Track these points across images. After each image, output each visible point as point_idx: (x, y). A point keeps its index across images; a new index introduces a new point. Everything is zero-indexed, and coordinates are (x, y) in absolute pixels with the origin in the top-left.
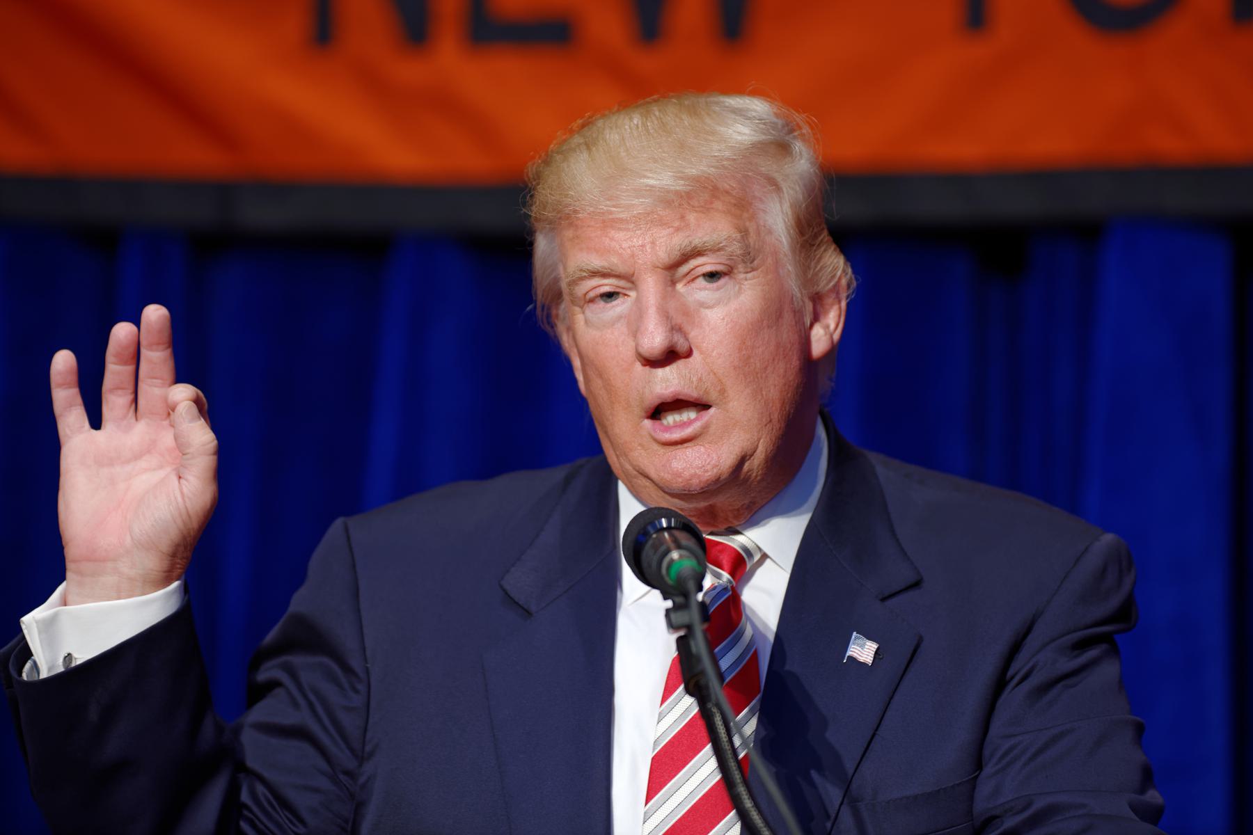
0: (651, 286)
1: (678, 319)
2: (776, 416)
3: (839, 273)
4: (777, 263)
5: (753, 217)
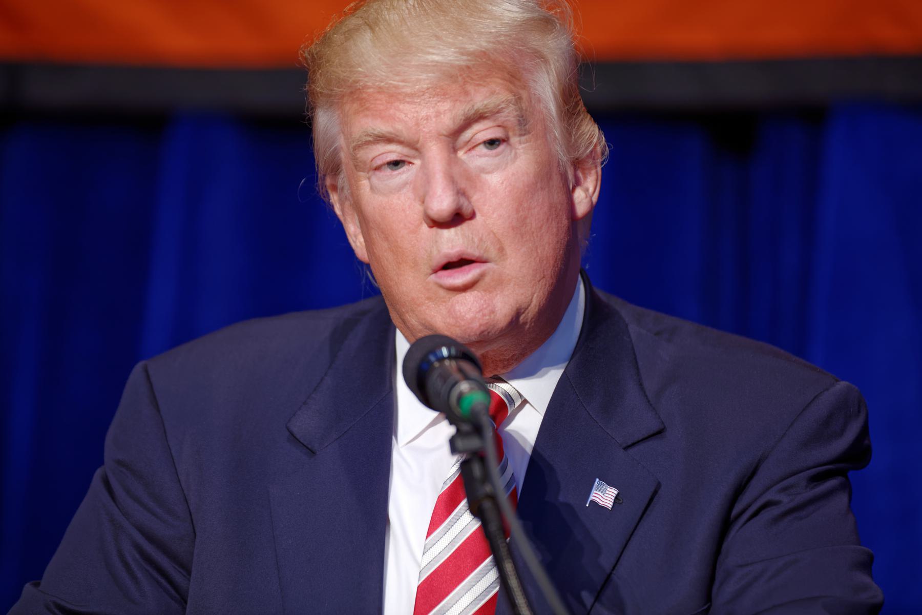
0: (435, 153)
1: (463, 184)
2: (549, 272)
3: (595, 140)
4: (546, 129)
5: (525, 87)
